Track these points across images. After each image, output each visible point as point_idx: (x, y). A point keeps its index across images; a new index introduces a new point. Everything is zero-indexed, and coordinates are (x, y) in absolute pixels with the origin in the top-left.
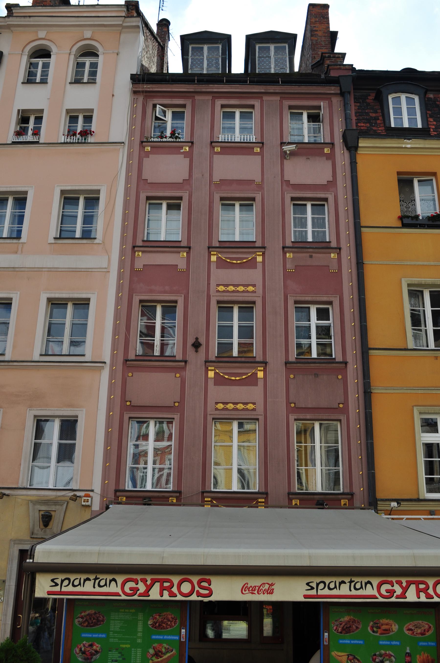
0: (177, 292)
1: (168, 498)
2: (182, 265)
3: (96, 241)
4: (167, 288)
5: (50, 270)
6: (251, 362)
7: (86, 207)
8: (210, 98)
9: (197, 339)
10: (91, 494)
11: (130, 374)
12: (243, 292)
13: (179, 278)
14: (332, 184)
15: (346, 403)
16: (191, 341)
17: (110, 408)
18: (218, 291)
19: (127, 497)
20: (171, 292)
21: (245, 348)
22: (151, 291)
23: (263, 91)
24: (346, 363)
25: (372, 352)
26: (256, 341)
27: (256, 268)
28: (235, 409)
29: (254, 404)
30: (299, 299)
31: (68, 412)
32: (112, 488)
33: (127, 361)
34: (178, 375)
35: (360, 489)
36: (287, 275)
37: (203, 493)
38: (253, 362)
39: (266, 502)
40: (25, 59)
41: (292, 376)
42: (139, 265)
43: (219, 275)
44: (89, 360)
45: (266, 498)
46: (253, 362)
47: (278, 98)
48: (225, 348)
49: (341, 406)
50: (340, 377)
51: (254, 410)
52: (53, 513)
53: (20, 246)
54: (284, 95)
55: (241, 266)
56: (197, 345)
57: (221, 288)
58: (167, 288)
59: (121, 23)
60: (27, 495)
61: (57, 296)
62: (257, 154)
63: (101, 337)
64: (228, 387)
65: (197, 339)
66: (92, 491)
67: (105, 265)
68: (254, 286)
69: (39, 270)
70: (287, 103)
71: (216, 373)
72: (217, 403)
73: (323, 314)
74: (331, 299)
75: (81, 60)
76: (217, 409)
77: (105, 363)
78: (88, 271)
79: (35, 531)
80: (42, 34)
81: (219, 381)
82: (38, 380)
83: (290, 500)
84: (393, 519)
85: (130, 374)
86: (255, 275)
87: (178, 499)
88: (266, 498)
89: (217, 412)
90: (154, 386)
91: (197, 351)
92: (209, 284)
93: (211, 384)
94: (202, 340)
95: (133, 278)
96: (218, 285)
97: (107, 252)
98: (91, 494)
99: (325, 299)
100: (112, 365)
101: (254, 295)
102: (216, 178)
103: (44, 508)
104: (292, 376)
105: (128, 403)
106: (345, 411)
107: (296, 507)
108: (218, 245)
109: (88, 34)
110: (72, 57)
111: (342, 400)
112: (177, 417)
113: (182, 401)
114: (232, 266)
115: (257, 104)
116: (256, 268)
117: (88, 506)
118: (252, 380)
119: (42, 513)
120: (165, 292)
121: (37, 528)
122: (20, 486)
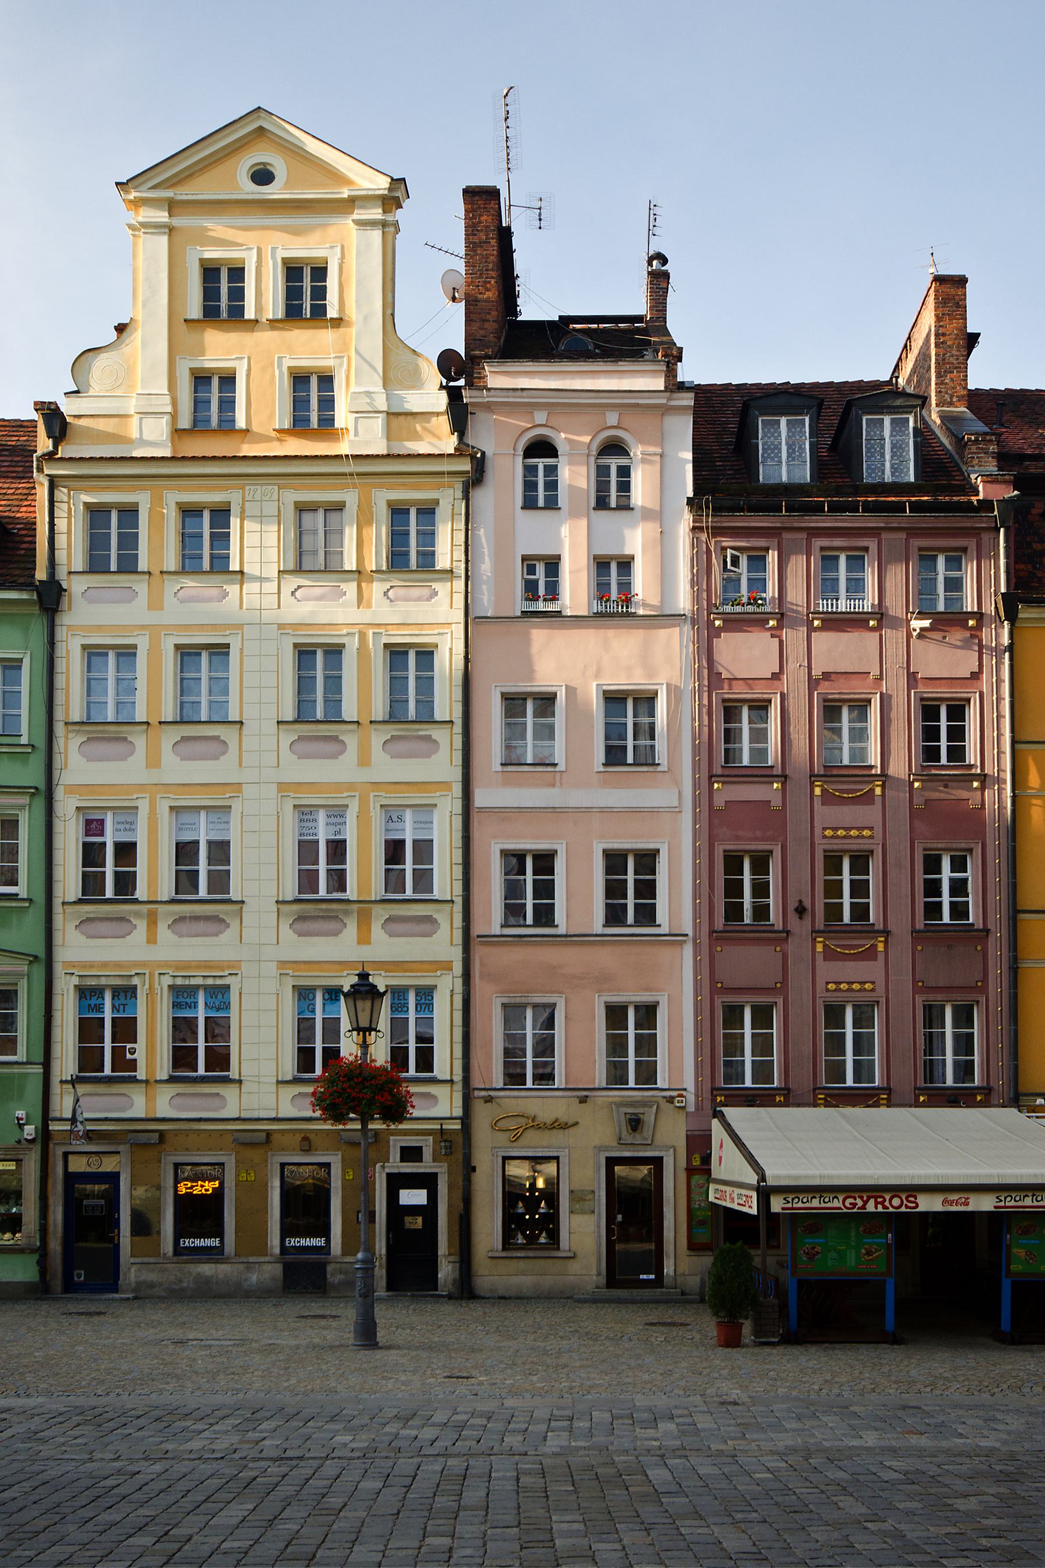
0: (772, 839)
1: (775, 1096)
2: (776, 802)
3: (659, 769)
4: (758, 833)
5: (603, 810)
6: (870, 932)
7: (754, 871)
8: (804, 535)
9: (800, 901)
10: (684, 1093)
11: (719, 949)
12: (858, 837)
13: (771, 819)
14: (976, 676)
15: (985, 979)
16: (792, 905)
17: (697, 992)
18: (825, 837)
19: (726, 1096)
20: (764, 839)
21: (860, 912)
22: (738, 838)
23: (882, 525)
24: (986, 931)
25: (1021, 916)
26: (873, 901)
27: (873, 804)
28: (850, 990)
29: (873, 983)
30: (928, 846)
31: (645, 998)
32: (707, 1086)
33: (714, 932)
34: (778, 949)
35: (1000, 1083)
36: (913, 813)
37: (814, 1090)
38: (872, 932)
39: (889, 1100)
40: (519, 459)
41: (919, 948)
42: (719, 802)
43: (826, 815)
44: (667, 932)
45: (889, 1095)
46: (872, 932)
47: (903, 535)
48: (834, 912)
49: (980, 984)
50: (979, 948)
51: (873, 990)
52: (641, 1116)
53: (558, 776)
54: (913, 532)
55: (855, 801)
56: (801, 910)
57: (828, 833)
58: (758, 833)
59: (664, 401)
60: (608, 1096)
61: (616, 846)
62: (873, 629)
63: (677, 898)
64: (840, 963)
65: (800, 901)
66: (685, 1090)
67: (675, 803)
68: (871, 829)
69: (588, 810)
70: (917, 543)
71: (825, 946)
72: (827, 983)
73: (958, 864)
74: (972, 846)
75: (605, 461)
76: (827, 990)
77: (686, 935)
78: (654, 811)
79: (623, 1136)
80: (541, 417)
81: (830, 955)
82: (605, 958)
83: (917, 1097)
84: (1037, 1117)
85: (719, 949)
86: (870, 814)
87: (786, 1097)
88: (889, 1095)
89: (829, 994)
90: (751, 963)
91: (801, 918)
92: (812, 827)
93: (819, 958)
94: (807, 904)
95: (713, 820)
96: (825, 829)
97: (677, 783)
98: (684, 1093)
99: (963, 846)
100: (695, 940)
101: (871, 841)
102: (816, 672)
103: (630, 1110)
104: (919, 948)
105: (719, 985)
106: (984, 990)
107: (923, 1105)
108: (822, 773)
109: (612, 418)
110: (592, 459)
111: (981, 977)
112: (780, 1002)
113: (784, 981)
114: (842, 801)
115: (872, 544)
116: (873, 804)
117: (684, 1107)
118: (870, 954)
119: (628, 1116)
120: (756, 839)
121: (624, 1133)
122: (597, 1086)
